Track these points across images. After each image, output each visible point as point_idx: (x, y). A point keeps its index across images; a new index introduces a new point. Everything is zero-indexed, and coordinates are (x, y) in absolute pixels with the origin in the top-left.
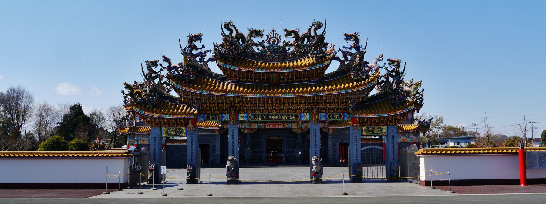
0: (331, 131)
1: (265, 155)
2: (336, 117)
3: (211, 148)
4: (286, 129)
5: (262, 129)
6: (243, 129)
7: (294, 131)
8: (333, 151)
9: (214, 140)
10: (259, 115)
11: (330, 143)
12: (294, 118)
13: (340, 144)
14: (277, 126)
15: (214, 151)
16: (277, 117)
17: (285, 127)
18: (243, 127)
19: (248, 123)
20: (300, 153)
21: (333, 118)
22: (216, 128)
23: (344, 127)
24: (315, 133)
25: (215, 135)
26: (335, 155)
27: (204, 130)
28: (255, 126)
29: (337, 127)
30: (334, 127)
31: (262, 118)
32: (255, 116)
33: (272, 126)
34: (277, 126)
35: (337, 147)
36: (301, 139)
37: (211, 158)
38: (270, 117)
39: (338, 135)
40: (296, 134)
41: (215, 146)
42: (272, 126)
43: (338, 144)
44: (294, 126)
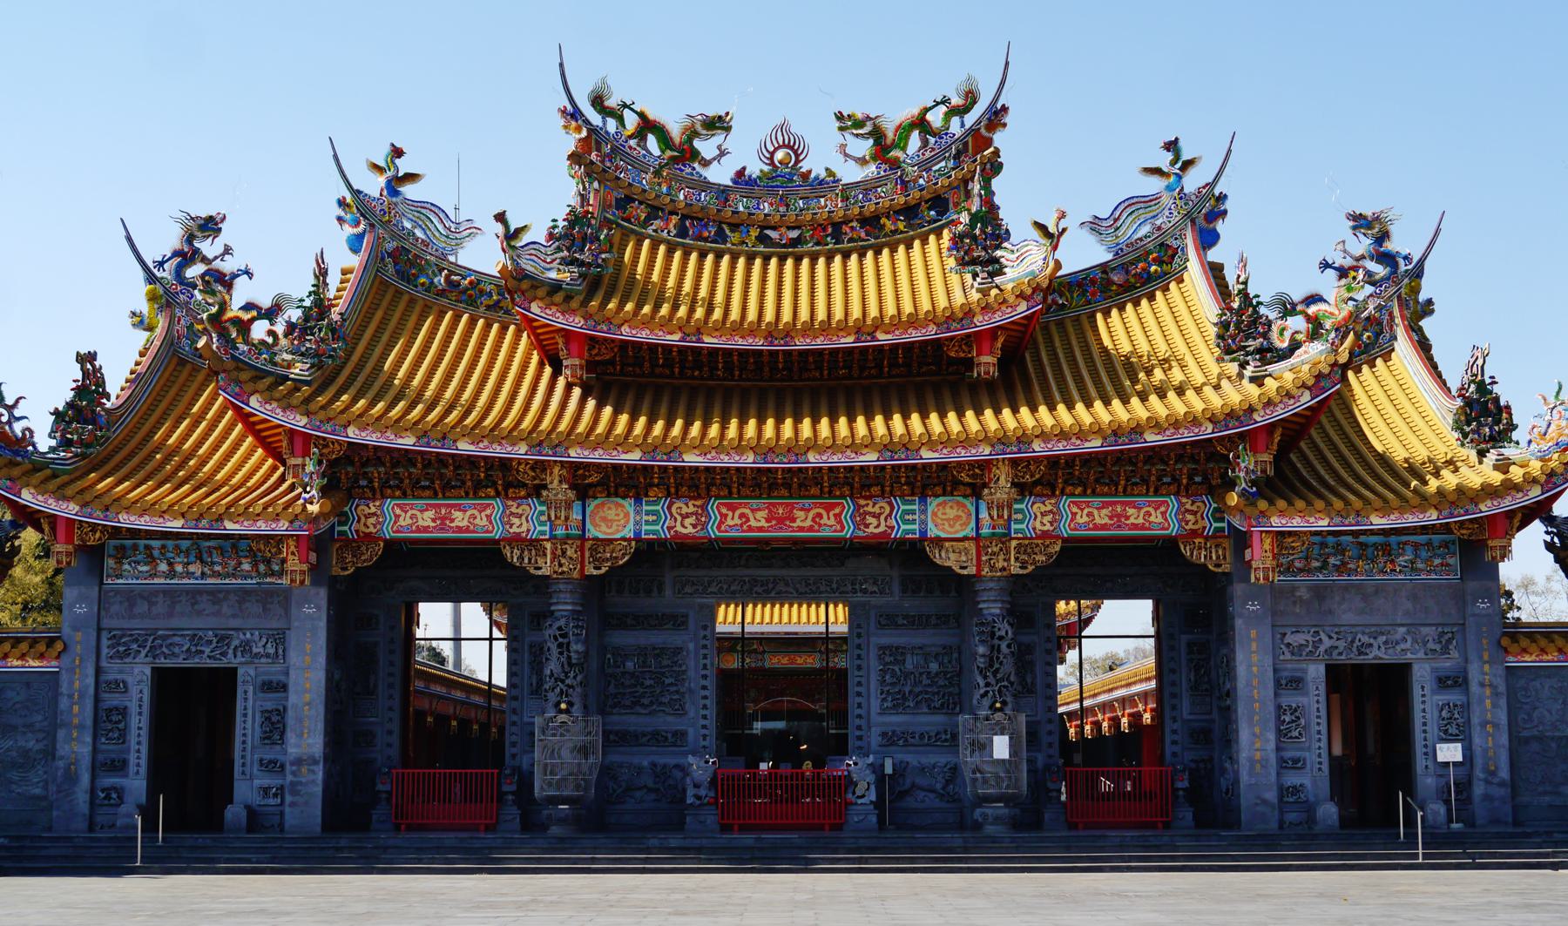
0: (1261, 556)
1: (701, 767)
4: (879, 548)
6: (516, 540)
7: (949, 559)
8: (1279, 732)
9: (279, 638)
11: (1251, 663)
13: (1335, 675)
14: (803, 519)
15: (274, 727)
17: (874, 527)
18: (519, 527)
19: (558, 488)
20: (1001, 747)
22: (282, 526)
23: (1378, 521)
25: (284, 596)
26: (1296, 764)
27: (197, 546)
28: (619, 522)
29: (1323, 524)
30: (1296, 523)
35: (1313, 699)
36: (1004, 628)
37: (247, 788)
39: (1320, 592)
40: (960, 587)
41: (284, 687)
42: (759, 519)
43: (1316, 673)
44: (944, 521)
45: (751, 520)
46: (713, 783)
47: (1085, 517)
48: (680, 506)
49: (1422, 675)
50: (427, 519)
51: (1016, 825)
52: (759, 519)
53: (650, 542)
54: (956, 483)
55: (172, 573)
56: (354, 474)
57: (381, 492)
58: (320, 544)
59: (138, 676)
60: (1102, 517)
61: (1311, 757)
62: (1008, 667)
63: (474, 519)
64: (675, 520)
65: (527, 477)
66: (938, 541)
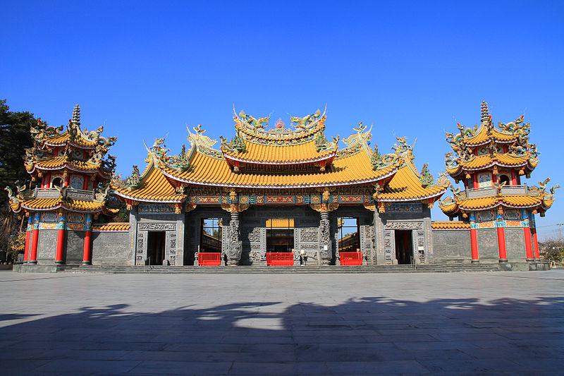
3: (168, 239)
4: (300, 206)
13: (397, 231)
33: (275, 200)
45: (274, 200)
46: (266, 256)
47: (345, 199)
49: (414, 233)
51: (330, 264)
52: (275, 200)
53: (252, 205)
54: (317, 192)
55: (152, 211)
56: (191, 189)
57: (197, 194)
58: (183, 205)
59: (145, 234)
61: (392, 250)
62: (327, 231)
63: (215, 200)
64: (259, 200)
65: (226, 190)
66: (313, 204)
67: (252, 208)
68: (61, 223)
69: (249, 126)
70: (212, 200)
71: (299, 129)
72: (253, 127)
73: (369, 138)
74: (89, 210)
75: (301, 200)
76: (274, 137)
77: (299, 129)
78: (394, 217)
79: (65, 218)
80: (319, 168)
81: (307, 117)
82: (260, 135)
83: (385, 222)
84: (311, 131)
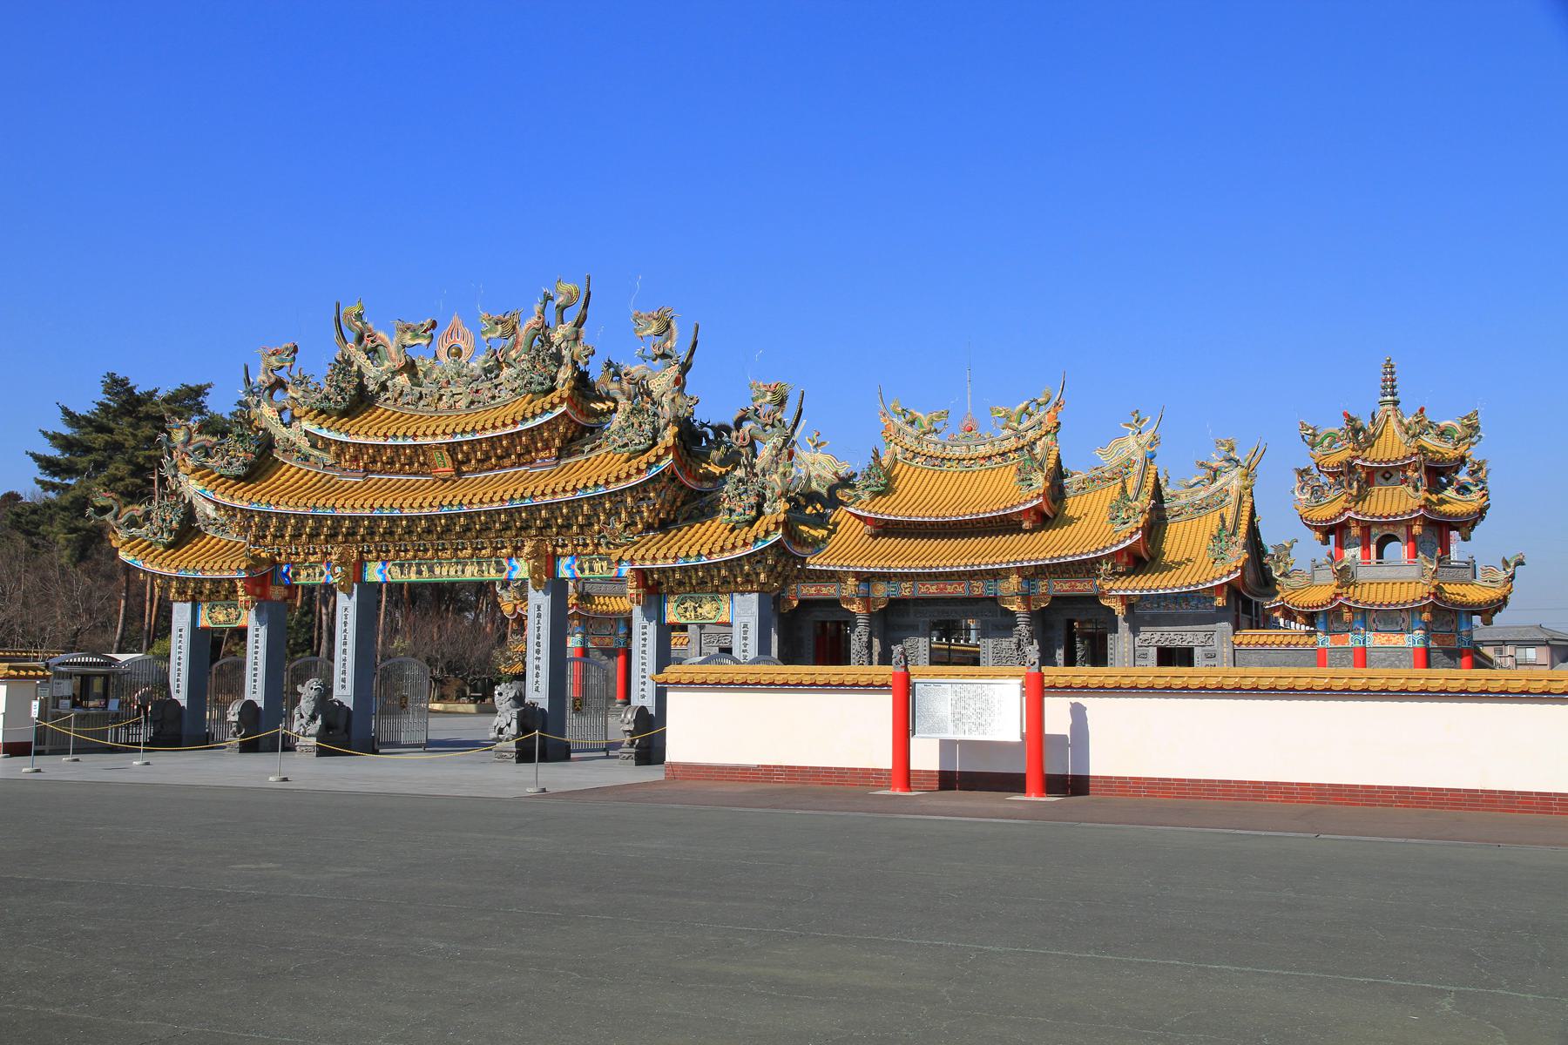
2: (597, 566)
5: (902, 602)
10: (410, 565)
12: (493, 571)
16: (452, 572)
17: (977, 592)
21: (592, 569)
24: (539, 616)
28: (881, 591)
31: (419, 572)
32: (401, 566)
33: (933, 589)
34: (950, 589)
38: (437, 570)
45: (932, 589)
48: (904, 585)
50: (813, 590)
52: (933, 589)
60: (1066, 587)
67: (896, 604)
68: (578, 636)
69: (908, 429)
70: (824, 590)
71: (1007, 432)
72: (915, 433)
73: (1151, 445)
74: (620, 612)
75: (979, 589)
76: (958, 452)
77: (1007, 432)
78: (1156, 621)
79: (584, 627)
80: (1021, 523)
81: (1022, 406)
82: (931, 450)
83: (1135, 631)
84: (1031, 435)
